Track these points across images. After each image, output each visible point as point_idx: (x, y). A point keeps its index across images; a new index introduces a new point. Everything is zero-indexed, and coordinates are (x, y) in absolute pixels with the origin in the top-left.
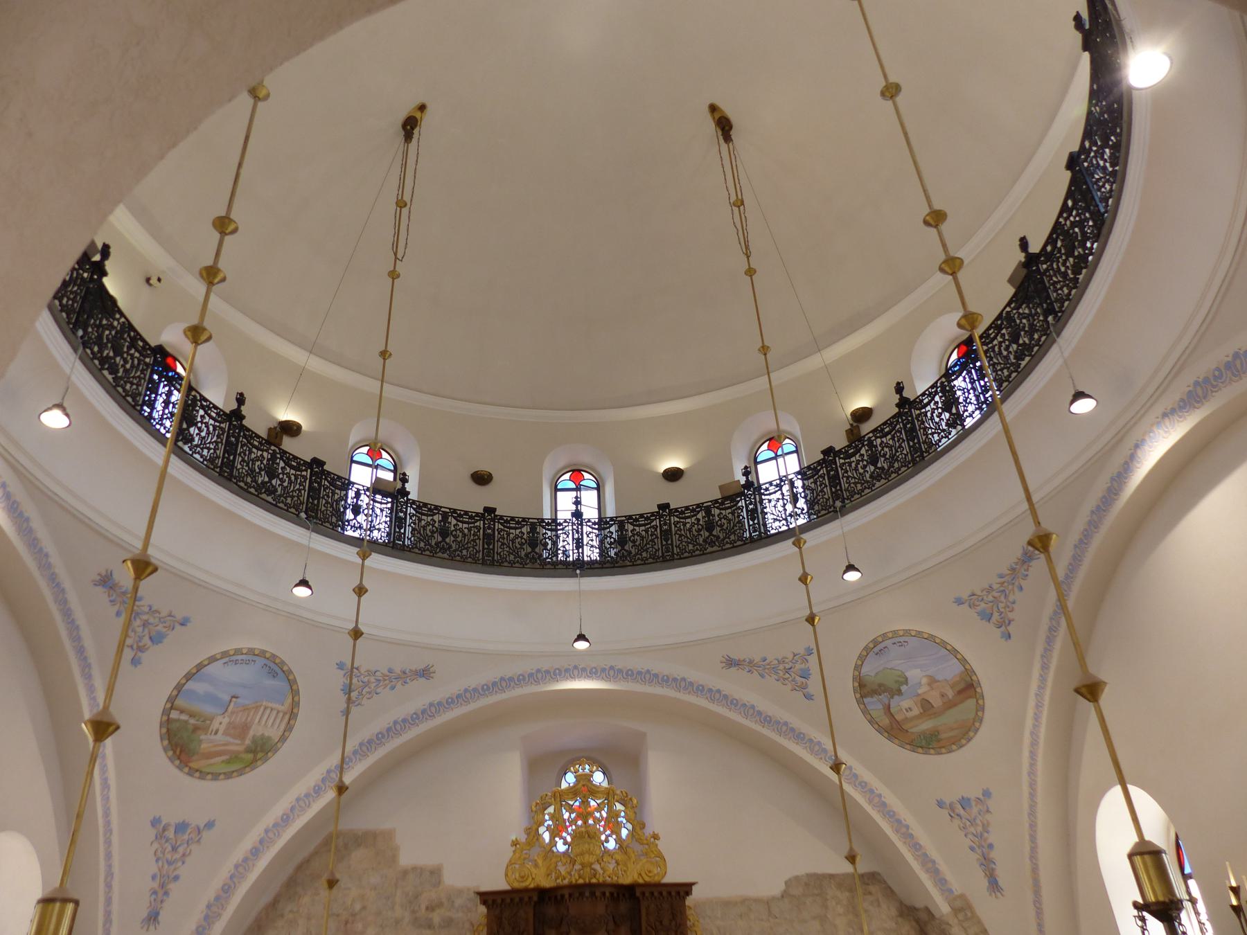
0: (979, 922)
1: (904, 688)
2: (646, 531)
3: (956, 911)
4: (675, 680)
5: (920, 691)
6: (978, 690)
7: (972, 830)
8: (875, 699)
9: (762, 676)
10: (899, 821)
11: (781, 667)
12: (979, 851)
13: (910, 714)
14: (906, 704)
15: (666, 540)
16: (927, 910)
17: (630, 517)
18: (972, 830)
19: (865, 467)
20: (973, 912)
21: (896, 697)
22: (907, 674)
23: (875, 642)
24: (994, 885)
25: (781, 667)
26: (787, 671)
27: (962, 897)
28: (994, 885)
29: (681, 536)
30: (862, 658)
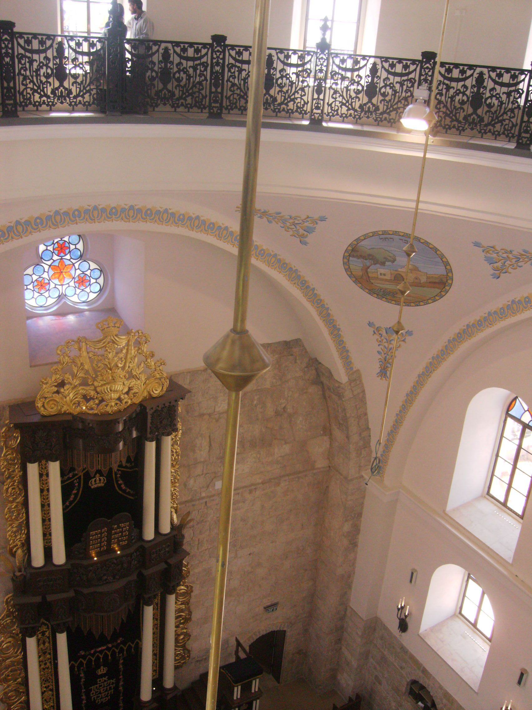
0: (363, 386)
1: (387, 263)
2: (195, 68)
3: (350, 382)
4: (190, 218)
5: (399, 270)
6: (447, 288)
7: (386, 345)
8: (359, 260)
9: (269, 222)
10: (335, 327)
11: (291, 221)
12: (384, 356)
13: (382, 277)
14: (382, 271)
15: (217, 87)
17: (177, 44)
18: (386, 345)
19: (462, 103)
21: (378, 265)
22: (398, 258)
23: (385, 232)
24: (384, 372)
25: (291, 221)
26: (294, 224)
27: (358, 371)
28: (384, 372)
29: (234, 85)
30: (366, 237)
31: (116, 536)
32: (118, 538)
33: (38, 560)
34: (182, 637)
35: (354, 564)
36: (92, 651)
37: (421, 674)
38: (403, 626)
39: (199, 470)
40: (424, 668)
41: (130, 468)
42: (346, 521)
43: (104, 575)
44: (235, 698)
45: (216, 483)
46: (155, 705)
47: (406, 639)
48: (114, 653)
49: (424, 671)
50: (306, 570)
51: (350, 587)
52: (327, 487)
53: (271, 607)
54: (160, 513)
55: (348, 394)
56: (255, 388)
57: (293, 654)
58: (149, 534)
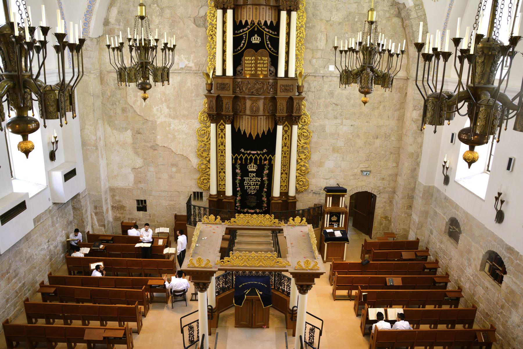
0: (424, 11)
3: (416, 5)
16: (404, 4)
20: (423, 7)
31: (260, 65)
32: (261, 67)
33: (219, 73)
34: (304, 168)
35: (421, 147)
36: (248, 152)
37: (454, 210)
38: (447, 180)
39: (319, 54)
40: (457, 205)
41: (274, 35)
42: (415, 109)
43: (252, 89)
44: (328, 206)
45: (330, 66)
46: (280, 201)
47: (449, 191)
48: (261, 159)
49: (457, 207)
50: (391, 153)
51: (418, 164)
52: (406, 93)
53: (366, 172)
54: (289, 65)
55: (413, 14)
56: (357, 11)
57: (381, 218)
58: (281, 73)
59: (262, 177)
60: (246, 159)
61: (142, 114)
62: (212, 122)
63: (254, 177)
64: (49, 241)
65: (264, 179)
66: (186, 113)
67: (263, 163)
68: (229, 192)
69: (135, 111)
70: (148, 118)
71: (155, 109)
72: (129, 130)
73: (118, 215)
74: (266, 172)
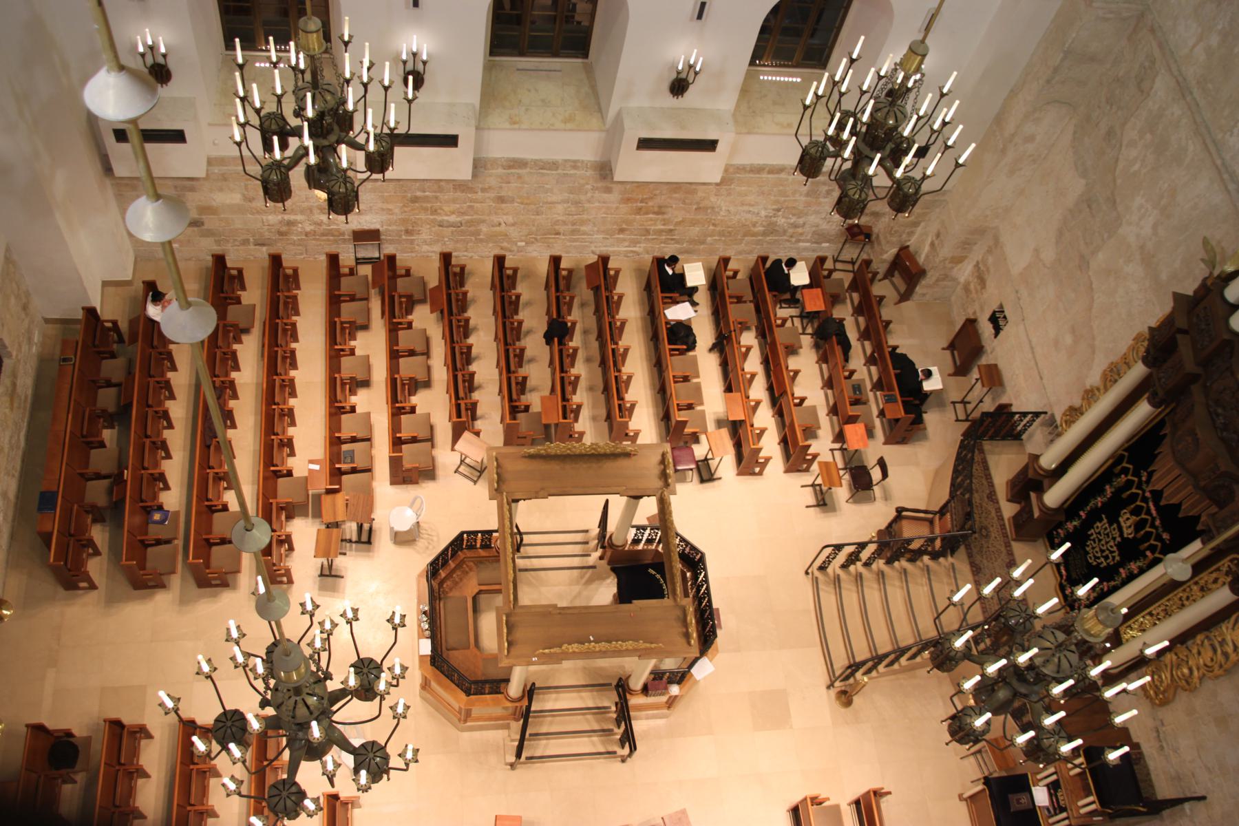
59: (1122, 564)
60: (1134, 497)
61: (1119, 181)
62: (1145, 361)
63: (1114, 539)
64: (779, 210)
65: (1121, 570)
66: (1164, 277)
67: (1143, 547)
68: (1055, 496)
69: (1117, 160)
70: (1118, 200)
71: (1139, 200)
72: (1083, 181)
73: (972, 287)
74: (1134, 566)
